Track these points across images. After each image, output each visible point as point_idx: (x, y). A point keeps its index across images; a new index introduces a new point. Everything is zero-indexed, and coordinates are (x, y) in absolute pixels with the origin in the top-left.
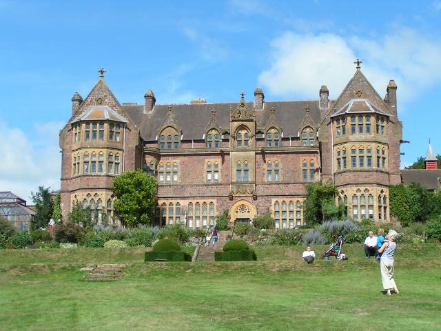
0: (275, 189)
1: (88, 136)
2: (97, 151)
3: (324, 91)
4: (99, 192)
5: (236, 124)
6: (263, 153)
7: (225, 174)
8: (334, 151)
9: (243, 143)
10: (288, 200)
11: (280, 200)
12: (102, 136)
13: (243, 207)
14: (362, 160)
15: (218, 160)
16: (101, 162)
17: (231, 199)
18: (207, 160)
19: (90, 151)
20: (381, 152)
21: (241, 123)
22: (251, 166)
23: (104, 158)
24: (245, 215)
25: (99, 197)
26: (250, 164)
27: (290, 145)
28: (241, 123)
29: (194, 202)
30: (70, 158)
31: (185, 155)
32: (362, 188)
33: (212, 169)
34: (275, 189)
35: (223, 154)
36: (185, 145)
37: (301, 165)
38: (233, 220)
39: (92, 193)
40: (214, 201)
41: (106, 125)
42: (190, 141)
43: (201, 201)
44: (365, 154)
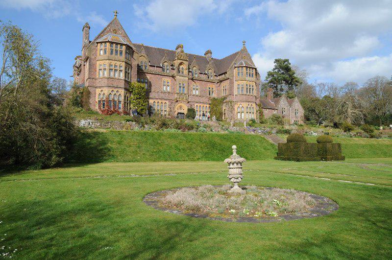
0: (197, 99)
1: (112, 53)
2: (118, 63)
3: (209, 52)
4: (120, 90)
5: (180, 61)
6: (192, 79)
7: (173, 87)
8: (236, 84)
9: (181, 73)
10: (202, 105)
11: (199, 105)
12: (121, 53)
13: (181, 107)
14: (250, 90)
15: (169, 80)
16: (121, 71)
17: (177, 101)
18: (163, 79)
19: (113, 63)
20: (248, 86)
21: (181, 61)
22: (186, 85)
23: (123, 68)
24: (182, 111)
25: (120, 93)
26: (185, 84)
27: (203, 77)
28: (181, 61)
29: (156, 101)
30: (95, 65)
31: (152, 74)
32: (250, 104)
33: (166, 83)
34: (197, 99)
35: (173, 77)
36: (152, 68)
37: (208, 88)
38: (176, 113)
39: (115, 90)
40: (167, 102)
41: (124, 47)
42: (154, 66)
43: (160, 101)
44: (251, 87)
